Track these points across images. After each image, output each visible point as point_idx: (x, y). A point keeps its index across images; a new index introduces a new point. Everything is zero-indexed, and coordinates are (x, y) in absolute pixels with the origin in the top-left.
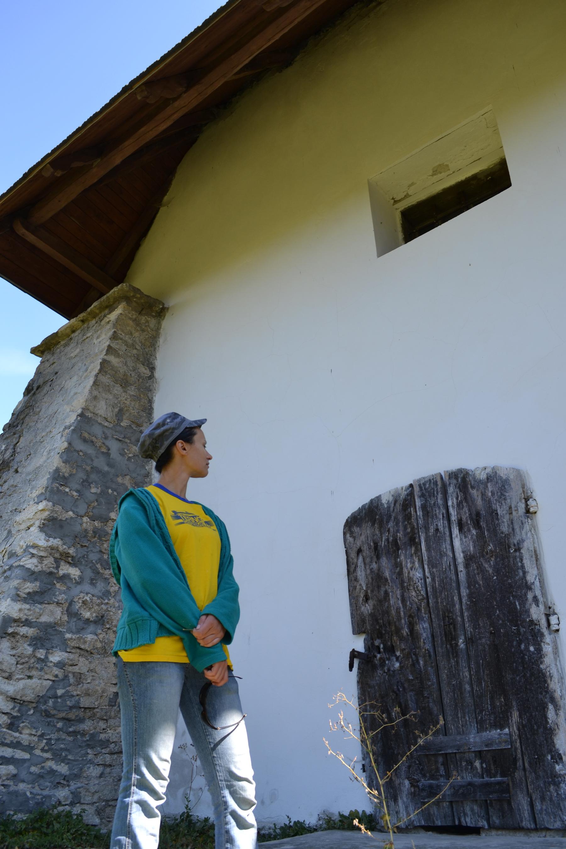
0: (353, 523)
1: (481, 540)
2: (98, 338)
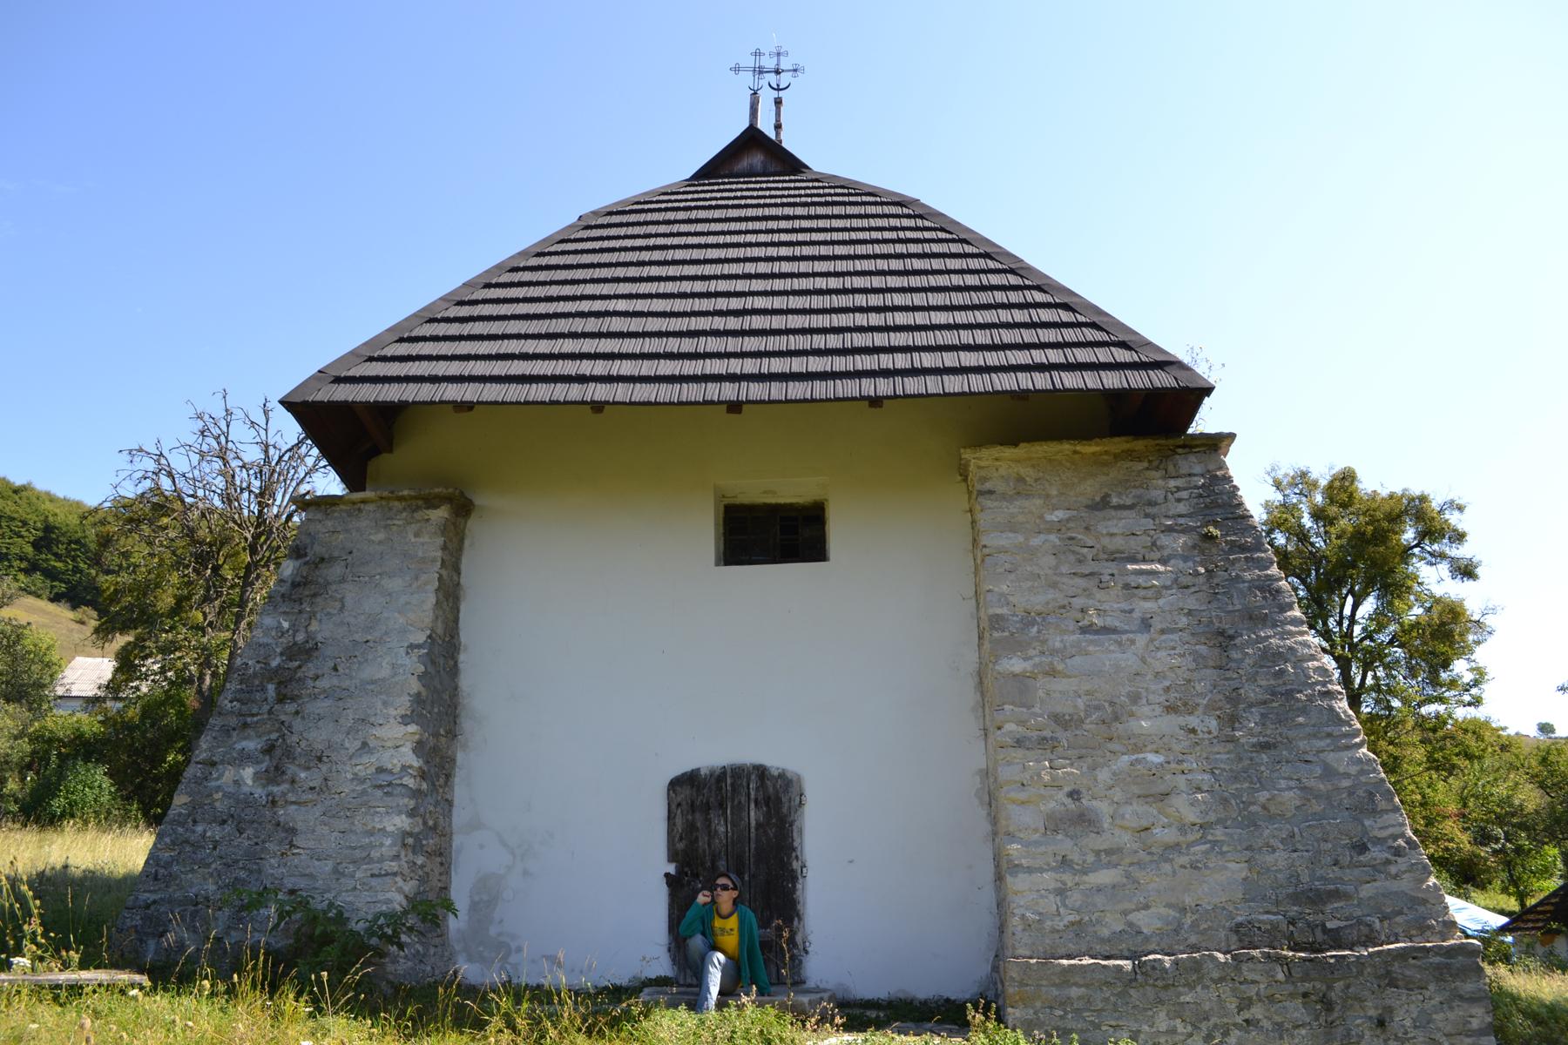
0: (675, 784)
1: (768, 815)
2: (416, 535)
